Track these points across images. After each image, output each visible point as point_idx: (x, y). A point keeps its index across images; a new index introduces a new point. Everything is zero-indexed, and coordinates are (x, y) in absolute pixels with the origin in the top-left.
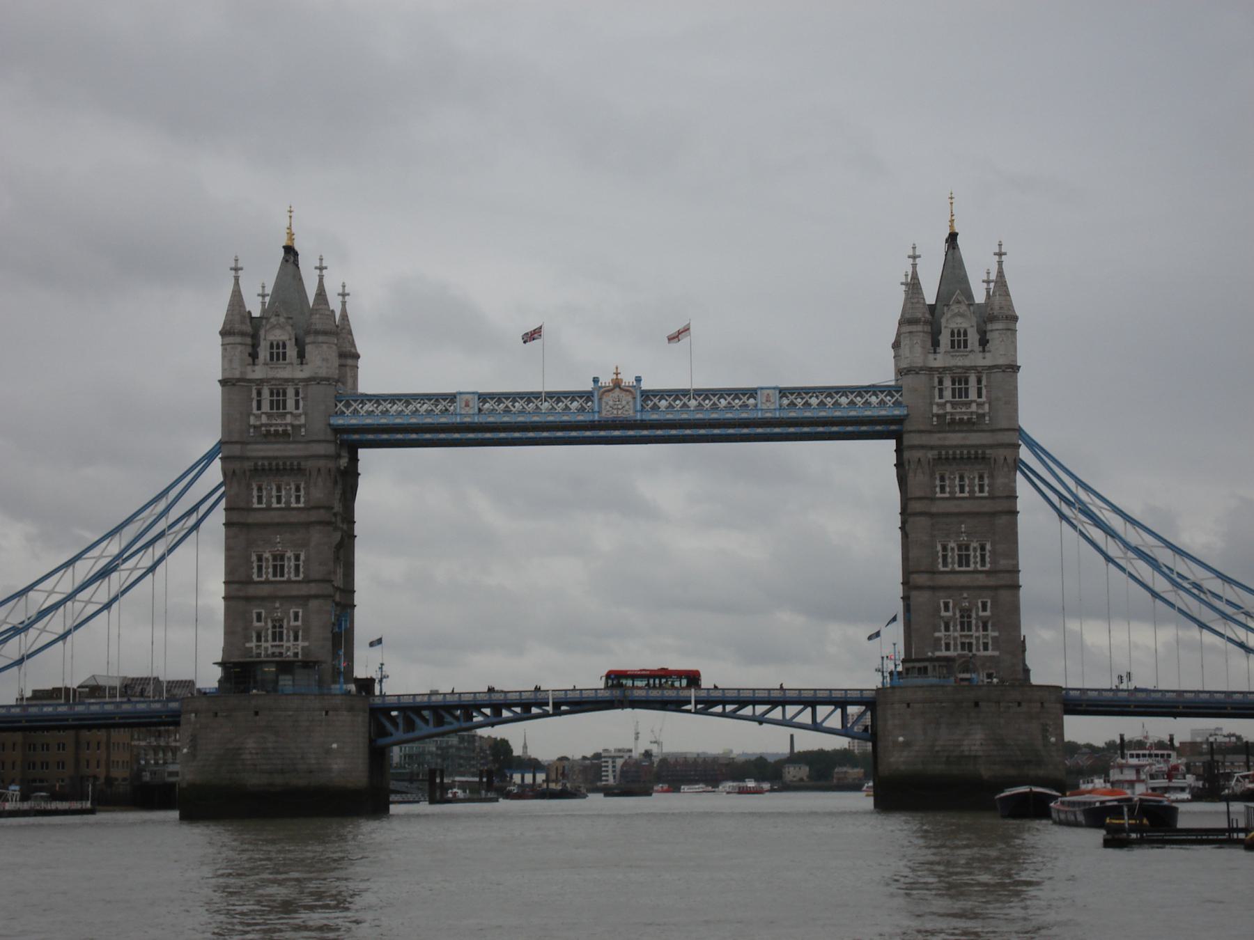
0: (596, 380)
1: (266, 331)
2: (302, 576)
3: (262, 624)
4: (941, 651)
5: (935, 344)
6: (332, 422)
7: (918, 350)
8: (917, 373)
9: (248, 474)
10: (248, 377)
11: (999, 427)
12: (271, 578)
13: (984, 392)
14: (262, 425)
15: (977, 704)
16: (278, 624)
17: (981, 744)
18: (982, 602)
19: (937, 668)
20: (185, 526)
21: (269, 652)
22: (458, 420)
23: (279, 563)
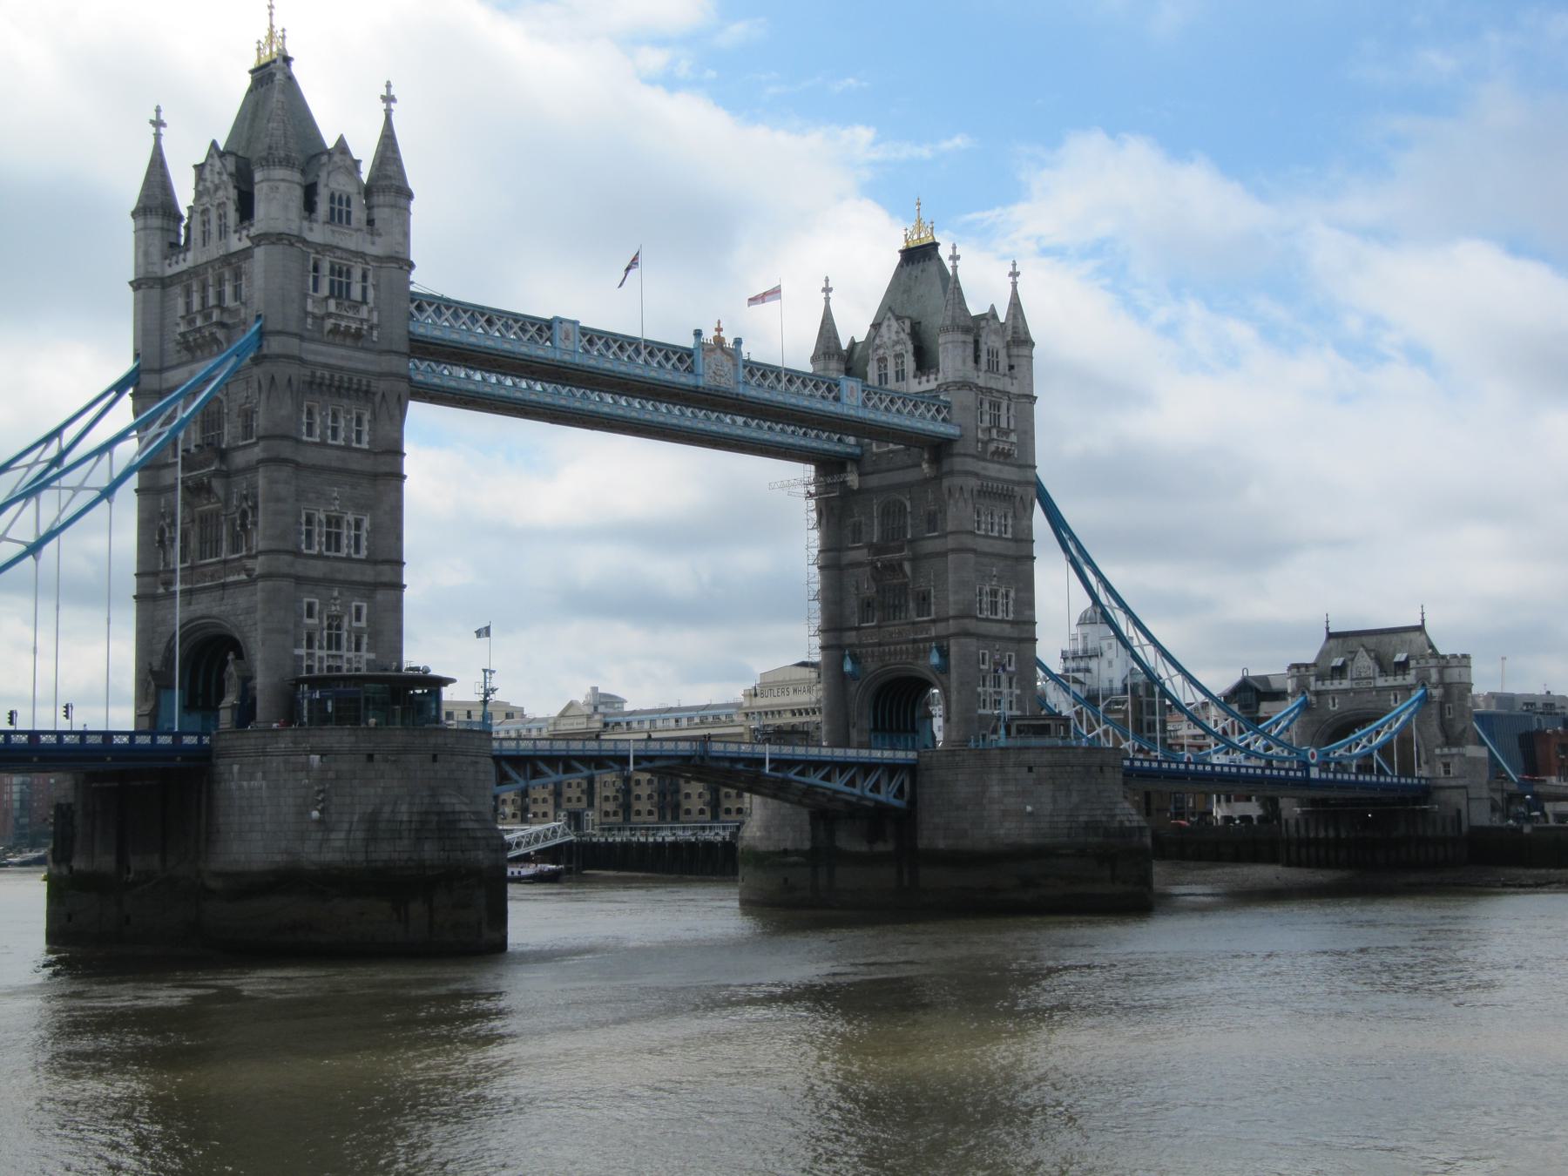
0: (698, 333)
1: (329, 174)
2: (363, 554)
3: (315, 621)
5: (977, 359)
6: (411, 329)
7: (970, 363)
8: (971, 390)
11: (1030, 462)
12: (326, 553)
14: (330, 315)
16: (335, 623)
20: (41, 459)
21: (325, 665)
22: (558, 356)
23: (334, 530)
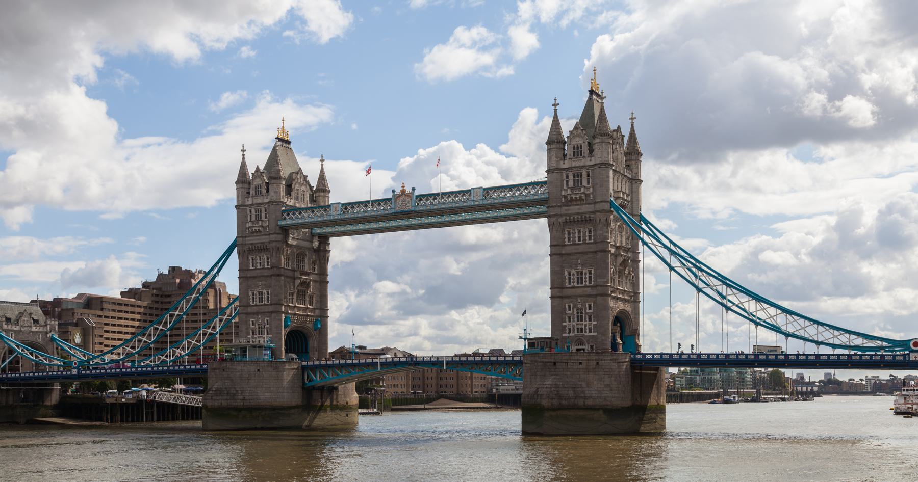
0: (393, 191)
4: (566, 333)
5: (565, 156)
6: (279, 223)
7: (554, 159)
8: (553, 173)
9: (247, 252)
10: (246, 204)
12: (258, 303)
13: (590, 181)
15: (555, 364)
17: (547, 388)
18: (589, 304)
19: (539, 343)
22: (332, 218)
23: (261, 296)
